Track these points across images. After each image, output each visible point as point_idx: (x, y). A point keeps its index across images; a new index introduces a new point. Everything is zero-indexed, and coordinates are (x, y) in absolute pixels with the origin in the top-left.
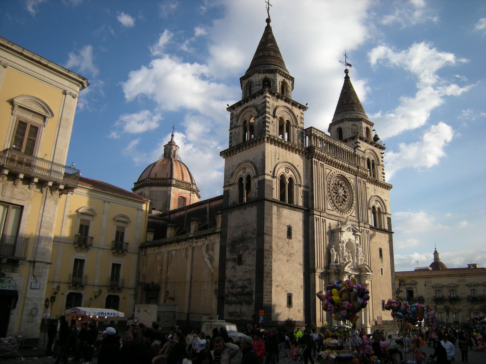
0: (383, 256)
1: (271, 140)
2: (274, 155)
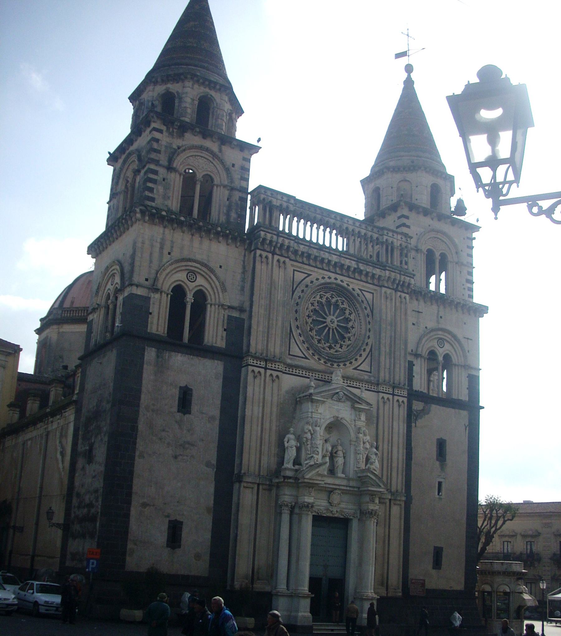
0: (449, 457)
1: (152, 216)
2: (158, 245)
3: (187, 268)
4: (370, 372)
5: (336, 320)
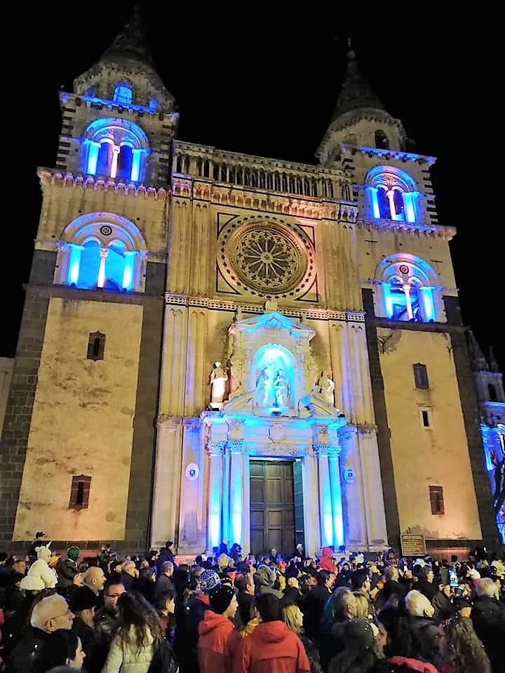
4: (318, 302)
5: (267, 253)
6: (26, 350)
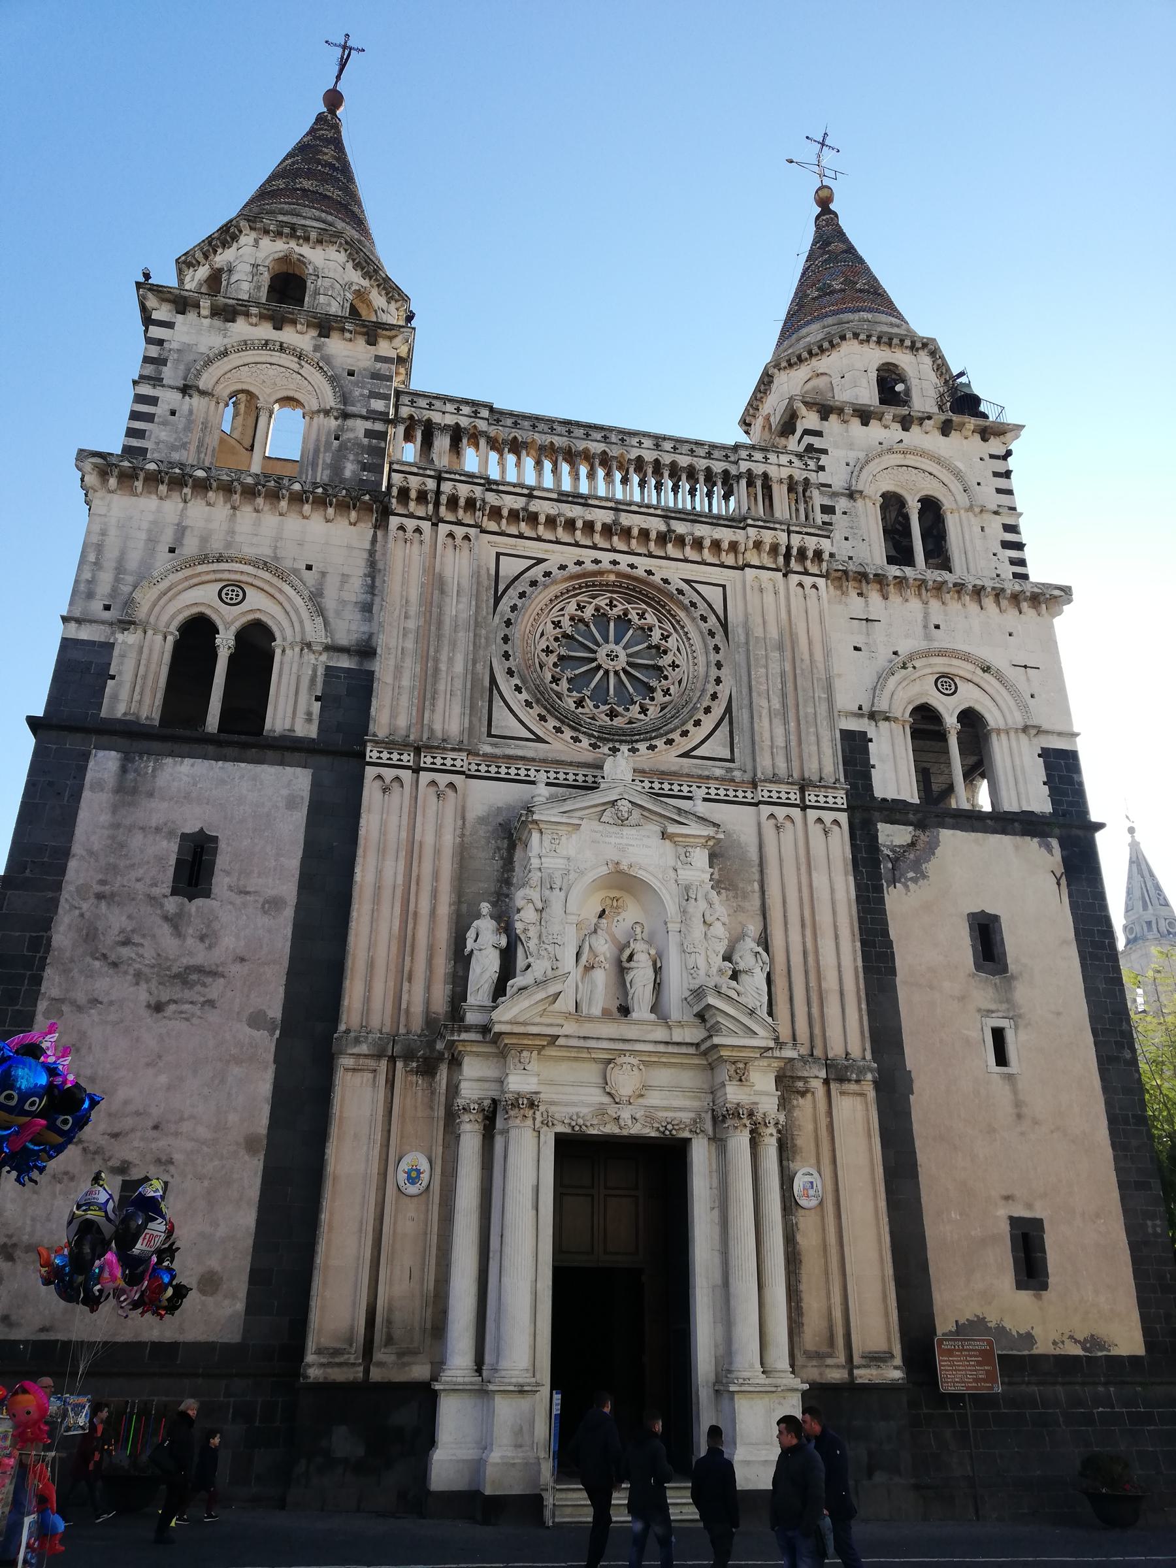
3: (219, 576)
4: (732, 760)
6: (28, 873)
